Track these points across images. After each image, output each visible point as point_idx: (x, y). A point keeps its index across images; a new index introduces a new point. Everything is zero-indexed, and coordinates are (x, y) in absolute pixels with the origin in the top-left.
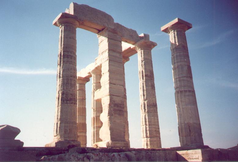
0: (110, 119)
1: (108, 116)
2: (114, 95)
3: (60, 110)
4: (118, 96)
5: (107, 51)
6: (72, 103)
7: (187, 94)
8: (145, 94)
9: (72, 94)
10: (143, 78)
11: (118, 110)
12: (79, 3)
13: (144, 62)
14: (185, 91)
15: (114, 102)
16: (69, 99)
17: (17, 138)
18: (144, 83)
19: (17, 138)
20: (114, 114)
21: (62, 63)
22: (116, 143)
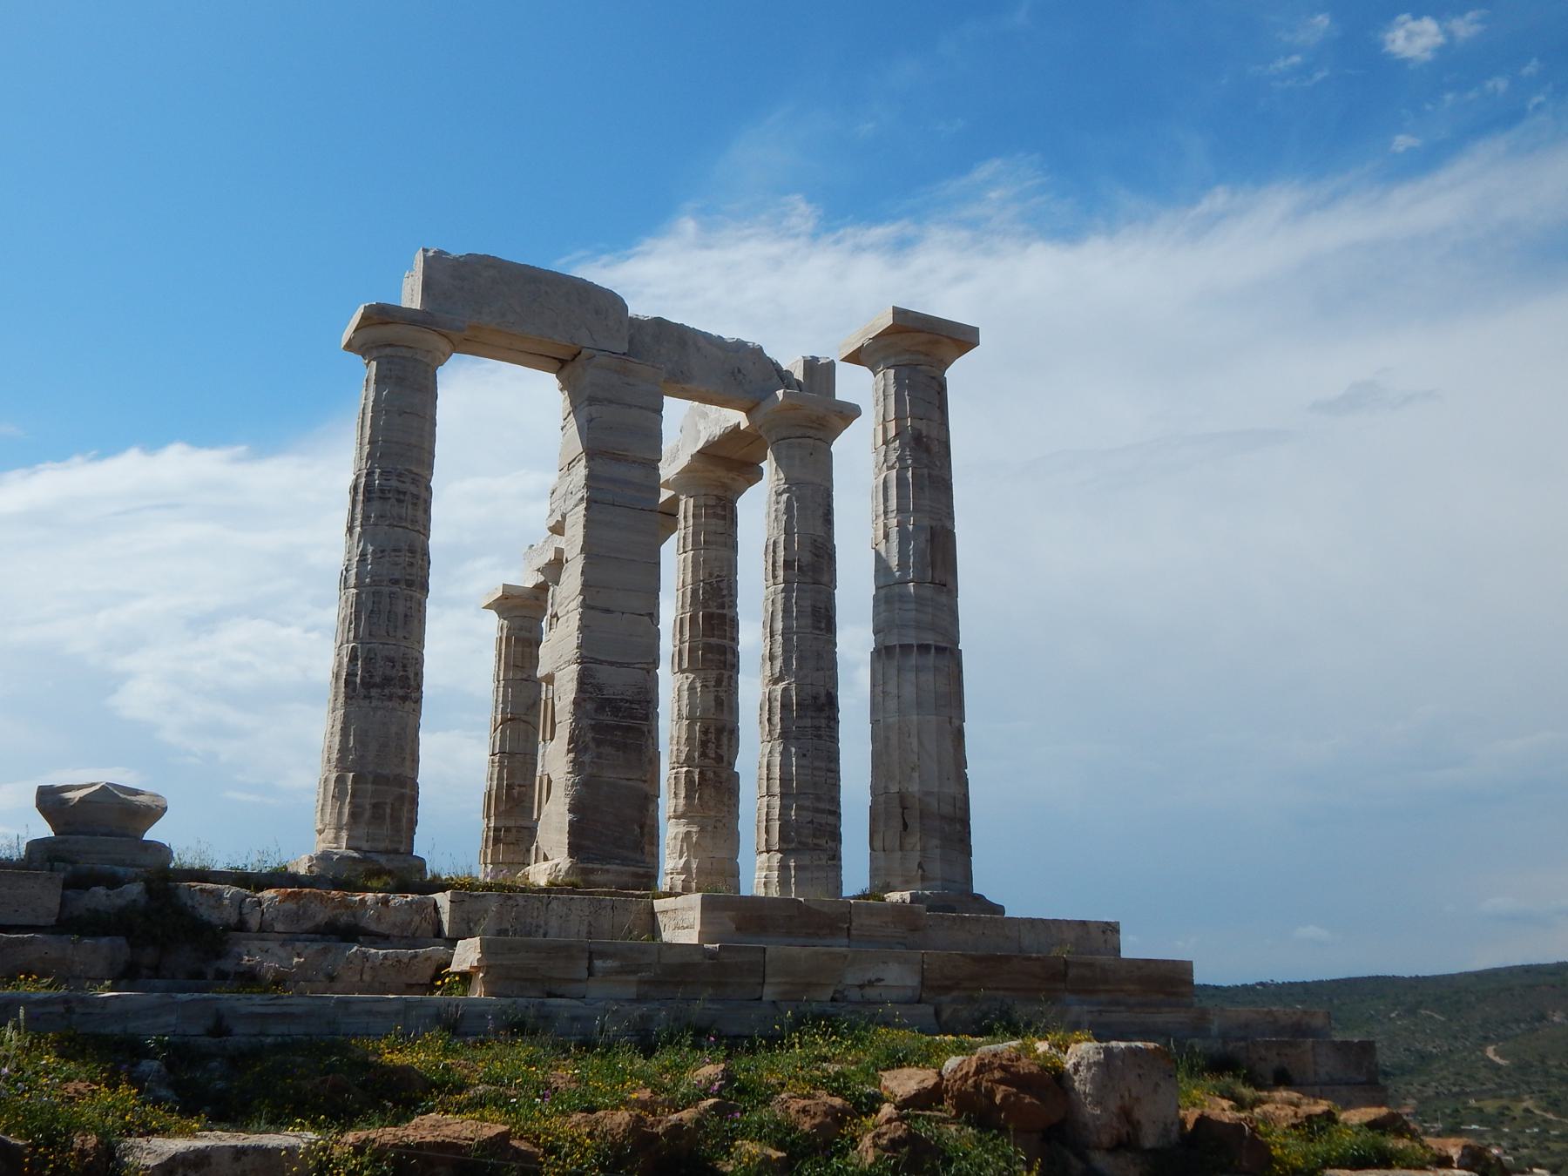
0: (577, 766)
1: (569, 751)
2: (601, 662)
3: (338, 726)
4: (622, 665)
5: (583, 462)
6: (390, 698)
7: (931, 659)
8: (779, 651)
9: (391, 660)
10: (775, 577)
11: (618, 727)
12: (457, 250)
13: (785, 496)
16: (378, 680)
17: (150, 835)
18: (780, 596)
19: (150, 835)
20: (592, 745)
21: (358, 523)
22: (592, 871)
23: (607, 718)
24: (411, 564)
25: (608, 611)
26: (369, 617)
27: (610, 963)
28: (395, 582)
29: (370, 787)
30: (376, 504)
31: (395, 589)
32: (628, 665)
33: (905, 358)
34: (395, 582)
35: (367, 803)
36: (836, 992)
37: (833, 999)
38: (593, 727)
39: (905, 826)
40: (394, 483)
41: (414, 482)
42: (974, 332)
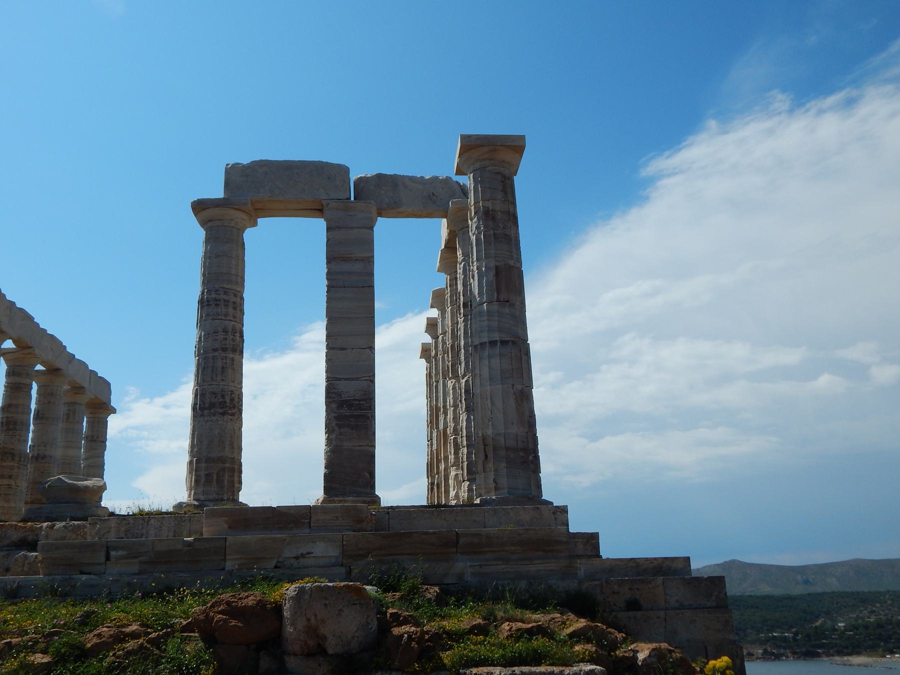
2: (340, 379)
4: (353, 379)
6: (214, 415)
9: (214, 393)
14: (493, 343)
15: (340, 395)
20: (336, 428)
23: (345, 411)
24: (226, 339)
25: (343, 349)
26: (202, 372)
27: (120, 553)
28: (215, 350)
29: (203, 465)
30: (206, 308)
31: (216, 354)
32: (357, 379)
33: (478, 165)
34: (215, 350)
35: (203, 473)
36: (278, 562)
37: (276, 567)
38: (336, 418)
39: (486, 457)
40: (213, 296)
41: (235, 296)
42: (522, 138)
